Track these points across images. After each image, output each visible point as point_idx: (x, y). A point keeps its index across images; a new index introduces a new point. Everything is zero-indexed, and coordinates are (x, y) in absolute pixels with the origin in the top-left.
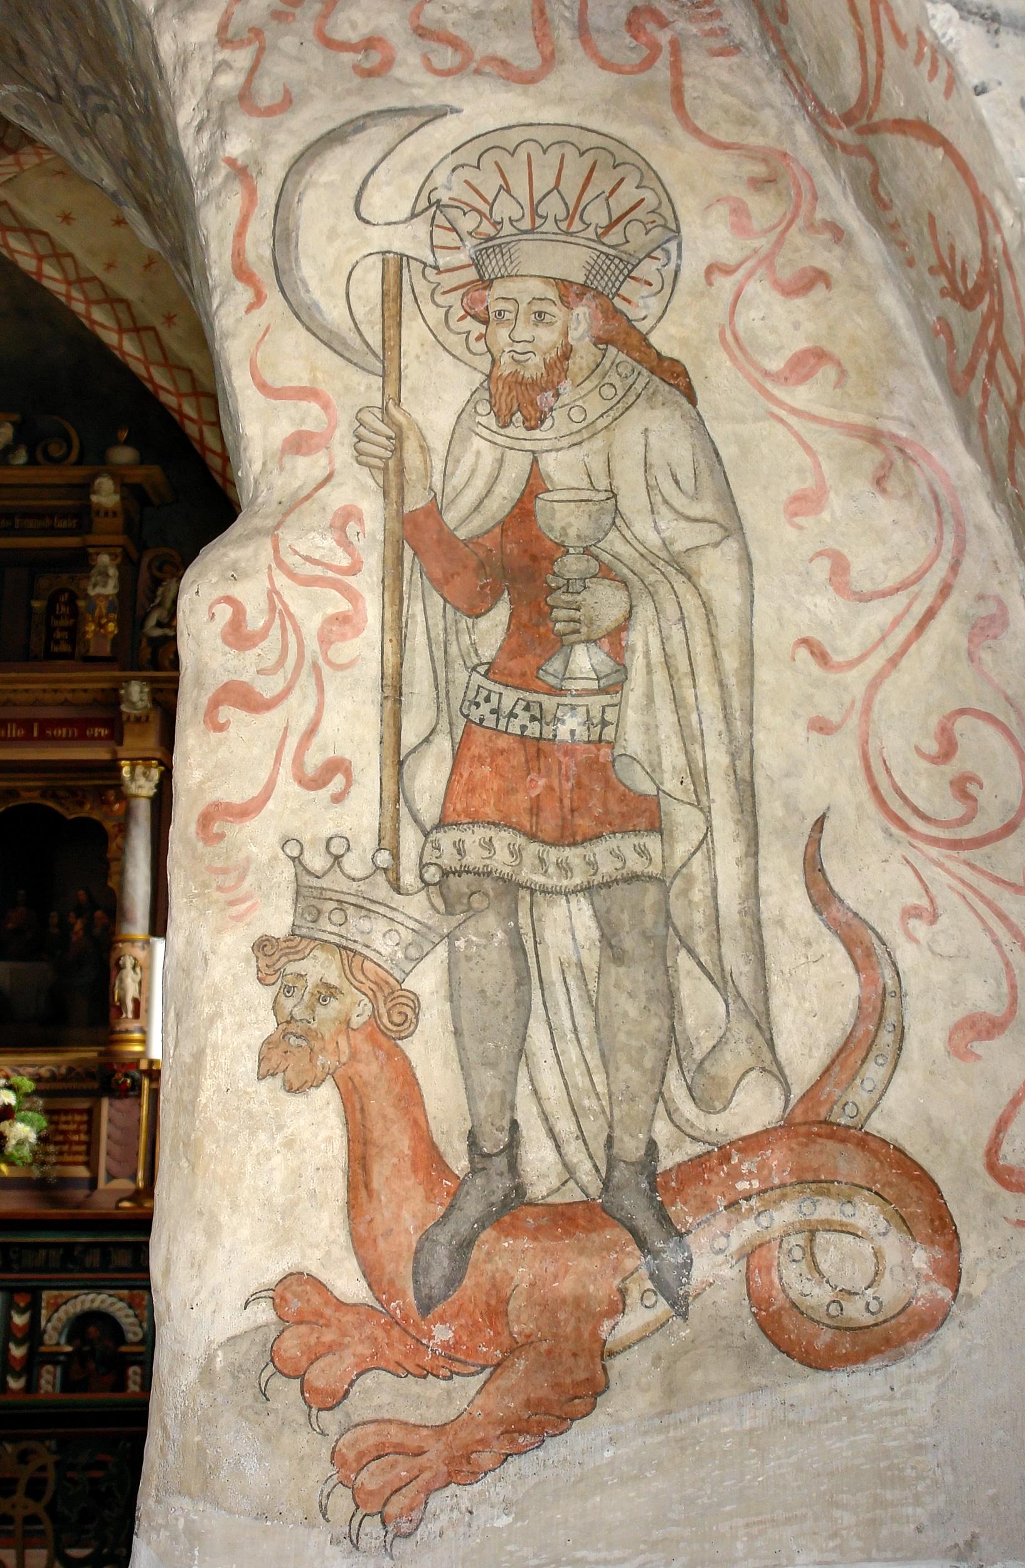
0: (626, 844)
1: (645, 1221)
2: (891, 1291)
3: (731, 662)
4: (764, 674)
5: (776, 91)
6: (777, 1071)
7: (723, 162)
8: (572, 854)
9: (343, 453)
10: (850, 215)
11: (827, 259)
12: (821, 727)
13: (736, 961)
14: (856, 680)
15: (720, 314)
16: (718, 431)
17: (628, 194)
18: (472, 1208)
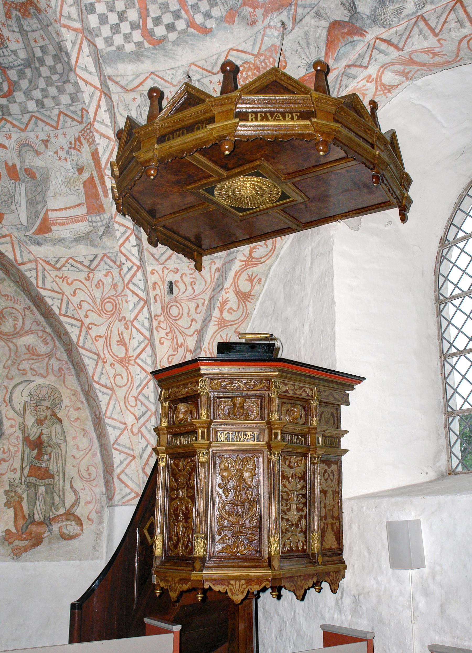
0: (49, 480)
1: (48, 524)
2: (75, 532)
3: (63, 458)
4: (67, 460)
5: (76, 382)
6: (65, 507)
7: (69, 391)
8: (43, 481)
9: (17, 428)
10: (84, 400)
11: (80, 406)
12: (73, 466)
13: (61, 494)
14: (78, 461)
15: (66, 412)
16: (65, 428)
17: (56, 395)
18: (29, 522)
